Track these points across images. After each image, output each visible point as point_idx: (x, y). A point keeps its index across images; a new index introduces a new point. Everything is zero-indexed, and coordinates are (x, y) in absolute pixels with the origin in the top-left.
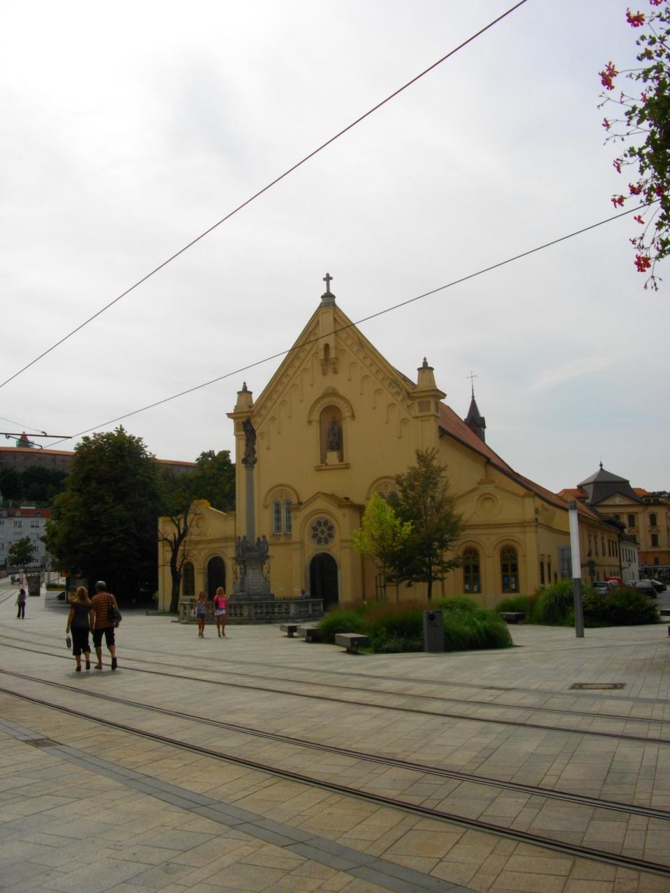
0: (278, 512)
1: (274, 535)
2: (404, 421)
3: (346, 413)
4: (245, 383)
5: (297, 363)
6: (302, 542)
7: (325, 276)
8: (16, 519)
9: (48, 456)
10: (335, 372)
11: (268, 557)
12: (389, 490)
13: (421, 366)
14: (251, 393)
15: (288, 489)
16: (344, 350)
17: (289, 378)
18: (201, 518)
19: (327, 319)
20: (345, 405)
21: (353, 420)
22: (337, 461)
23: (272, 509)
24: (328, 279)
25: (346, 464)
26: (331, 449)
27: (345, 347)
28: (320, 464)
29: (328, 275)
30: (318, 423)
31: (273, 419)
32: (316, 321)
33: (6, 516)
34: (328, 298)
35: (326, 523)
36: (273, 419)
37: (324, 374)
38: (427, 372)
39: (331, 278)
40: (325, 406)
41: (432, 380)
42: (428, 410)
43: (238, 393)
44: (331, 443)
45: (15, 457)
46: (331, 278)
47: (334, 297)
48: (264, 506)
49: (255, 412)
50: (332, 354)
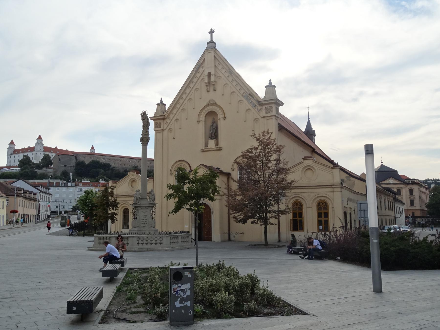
3: (220, 116)
4: (161, 99)
5: (192, 85)
7: (210, 31)
8: (78, 187)
9: (102, 157)
10: (215, 90)
11: (155, 204)
13: (268, 84)
14: (165, 105)
16: (220, 76)
18: (134, 181)
19: (210, 56)
20: (220, 111)
21: (225, 120)
22: (215, 145)
24: (212, 32)
25: (220, 148)
26: (211, 138)
27: (221, 75)
29: (211, 29)
30: (204, 122)
33: (74, 185)
34: (212, 44)
36: (177, 120)
37: (208, 92)
38: (271, 88)
40: (209, 111)
41: (274, 93)
42: (271, 112)
43: (157, 104)
44: (211, 134)
45: (85, 157)
46: (214, 32)
47: (215, 44)
49: (166, 116)
50: (213, 79)
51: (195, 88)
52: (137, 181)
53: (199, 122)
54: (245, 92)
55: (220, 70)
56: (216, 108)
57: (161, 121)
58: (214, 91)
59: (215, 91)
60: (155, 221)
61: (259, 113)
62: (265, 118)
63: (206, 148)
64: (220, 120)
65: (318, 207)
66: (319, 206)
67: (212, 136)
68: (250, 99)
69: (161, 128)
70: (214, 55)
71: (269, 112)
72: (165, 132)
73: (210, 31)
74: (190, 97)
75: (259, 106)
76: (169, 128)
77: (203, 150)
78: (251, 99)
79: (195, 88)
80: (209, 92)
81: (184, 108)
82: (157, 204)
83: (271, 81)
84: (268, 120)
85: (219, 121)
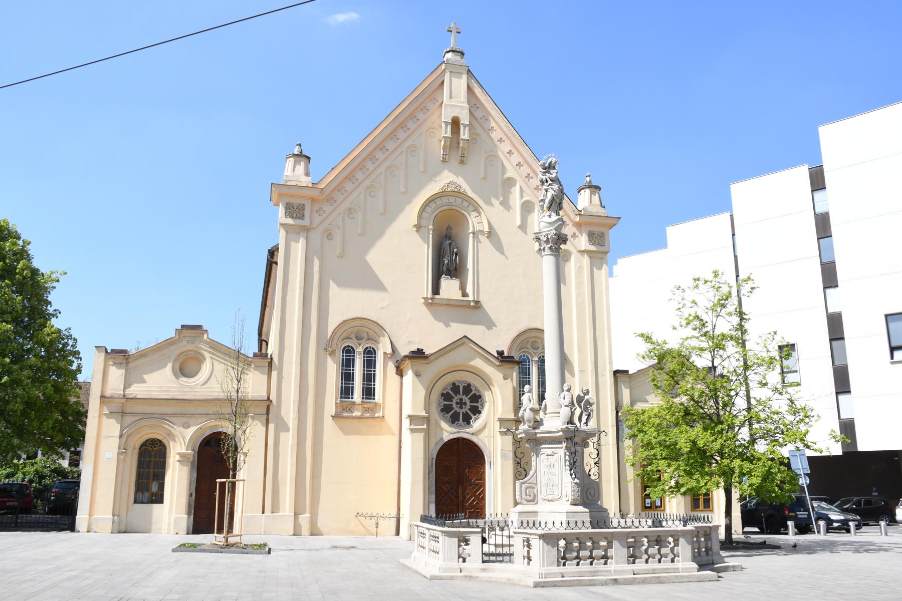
0: (348, 363)
17: (387, 153)
23: (339, 355)
32: (441, 81)
44: (448, 264)
50: (464, 134)
55: (479, 119)
69: (306, 222)
70: (468, 83)
71: (597, 241)
72: (316, 235)
74: (392, 162)
76: (325, 225)
79: (409, 142)
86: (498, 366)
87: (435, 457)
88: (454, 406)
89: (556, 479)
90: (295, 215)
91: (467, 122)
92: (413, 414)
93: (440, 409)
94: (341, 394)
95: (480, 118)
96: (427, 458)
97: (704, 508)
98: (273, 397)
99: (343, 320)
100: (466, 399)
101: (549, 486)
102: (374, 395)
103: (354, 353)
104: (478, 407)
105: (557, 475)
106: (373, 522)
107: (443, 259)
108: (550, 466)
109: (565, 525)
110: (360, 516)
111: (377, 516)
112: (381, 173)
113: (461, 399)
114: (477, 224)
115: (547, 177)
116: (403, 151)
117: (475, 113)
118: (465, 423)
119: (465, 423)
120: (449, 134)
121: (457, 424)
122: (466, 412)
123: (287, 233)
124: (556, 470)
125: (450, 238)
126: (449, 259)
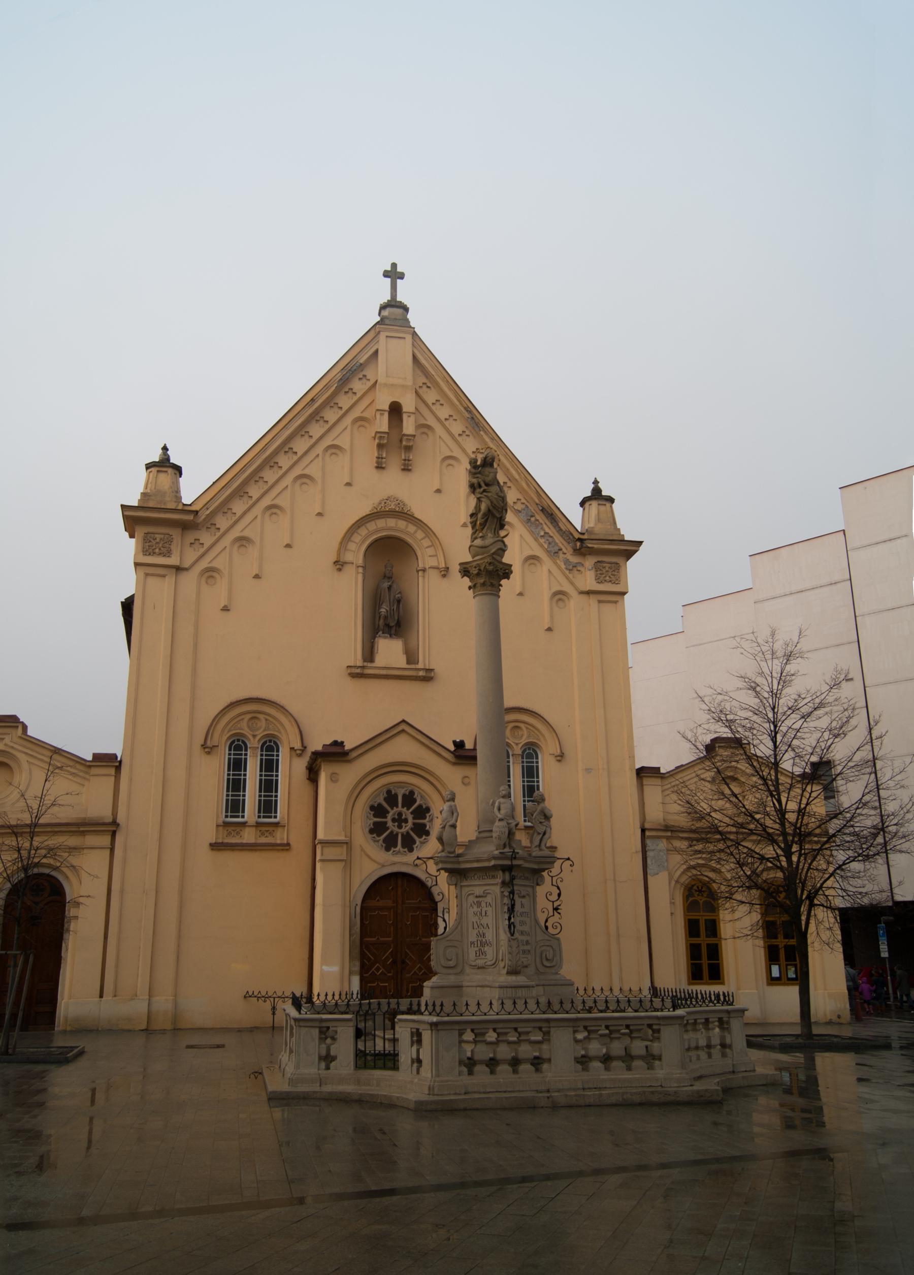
0: (237, 765)
1: (226, 824)
2: (559, 596)
5: (316, 430)
6: (347, 844)
10: (407, 468)
12: (524, 741)
15: (272, 711)
16: (429, 427)
21: (444, 576)
24: (394, 274)
27: (431, 421)
28: (360, 663)
29: (394, 266)
30: (361, 570)
31: (243, 541)
35: (409, 799)
36: (243, 541)
37: (380, 467)
39: (401, 276)
44: (386, 618)
46: (401, 276)
48: (204, 746)
50: (409, 426)
51: (327, 442)
52: (25, 766)
53: (342, 565)
54: (523, 501)
55: (431, 405)
56: (412, 528)
57: (176, 533)
58: (403, 470)
59: (406, 473)
60: (558, 939)
61: (570, 576)
62: (591, 596)
63: (365, 664)
64: (426, 574)
65: (687, 901)
66: (691, 899)
67: (387, 625)
68: (537, 524)
69: (174, 560)
71: (608, 578)
72: (189, 580)
73: (389, 269)
75: (572, 551)
76: (204, 564)
77: (358, 671)
78: (545, 526)
79: (327, 442)
80: (383, 468)
81: (277, 502)
82: (569, 862)
83: (599, 485)
84: (602, 605)
85: (424, 577)
86: (454, 764)
87: (359, 902)
88: (390, 824)
89: (490, 936)
90: (157, 550)
91: (412, 409)
92: (326, 838)
93: (367, 830)
94: (227, 811)
95: (433, 404)
96: (348, 904)
97: (710, 979)
98: (120, 819)
99: (229, 703)
100: (408, 814)
101: (479, 945)
102: (276, 812)
103: (246, 750)
104: (425, 825)
105: (490, 926)
106: (268, 1005)
107: (379, 609)
108: (481, 913)
109: (496, 1006)
110: (250, 996)
111: (275, 996)
112: (287, 486)
113: (400, 814)
114: (429, 558)
115: (480, 480)
116: (318, 455)
117: (425, 397)
118: (406, 850)
119: (406, 850)
120: (385, 428)
121: (394, 851)
122: (408, 833)
123: (147, 575)
124: (489, 920)
125: (390, 578)
126: (388, 609)
